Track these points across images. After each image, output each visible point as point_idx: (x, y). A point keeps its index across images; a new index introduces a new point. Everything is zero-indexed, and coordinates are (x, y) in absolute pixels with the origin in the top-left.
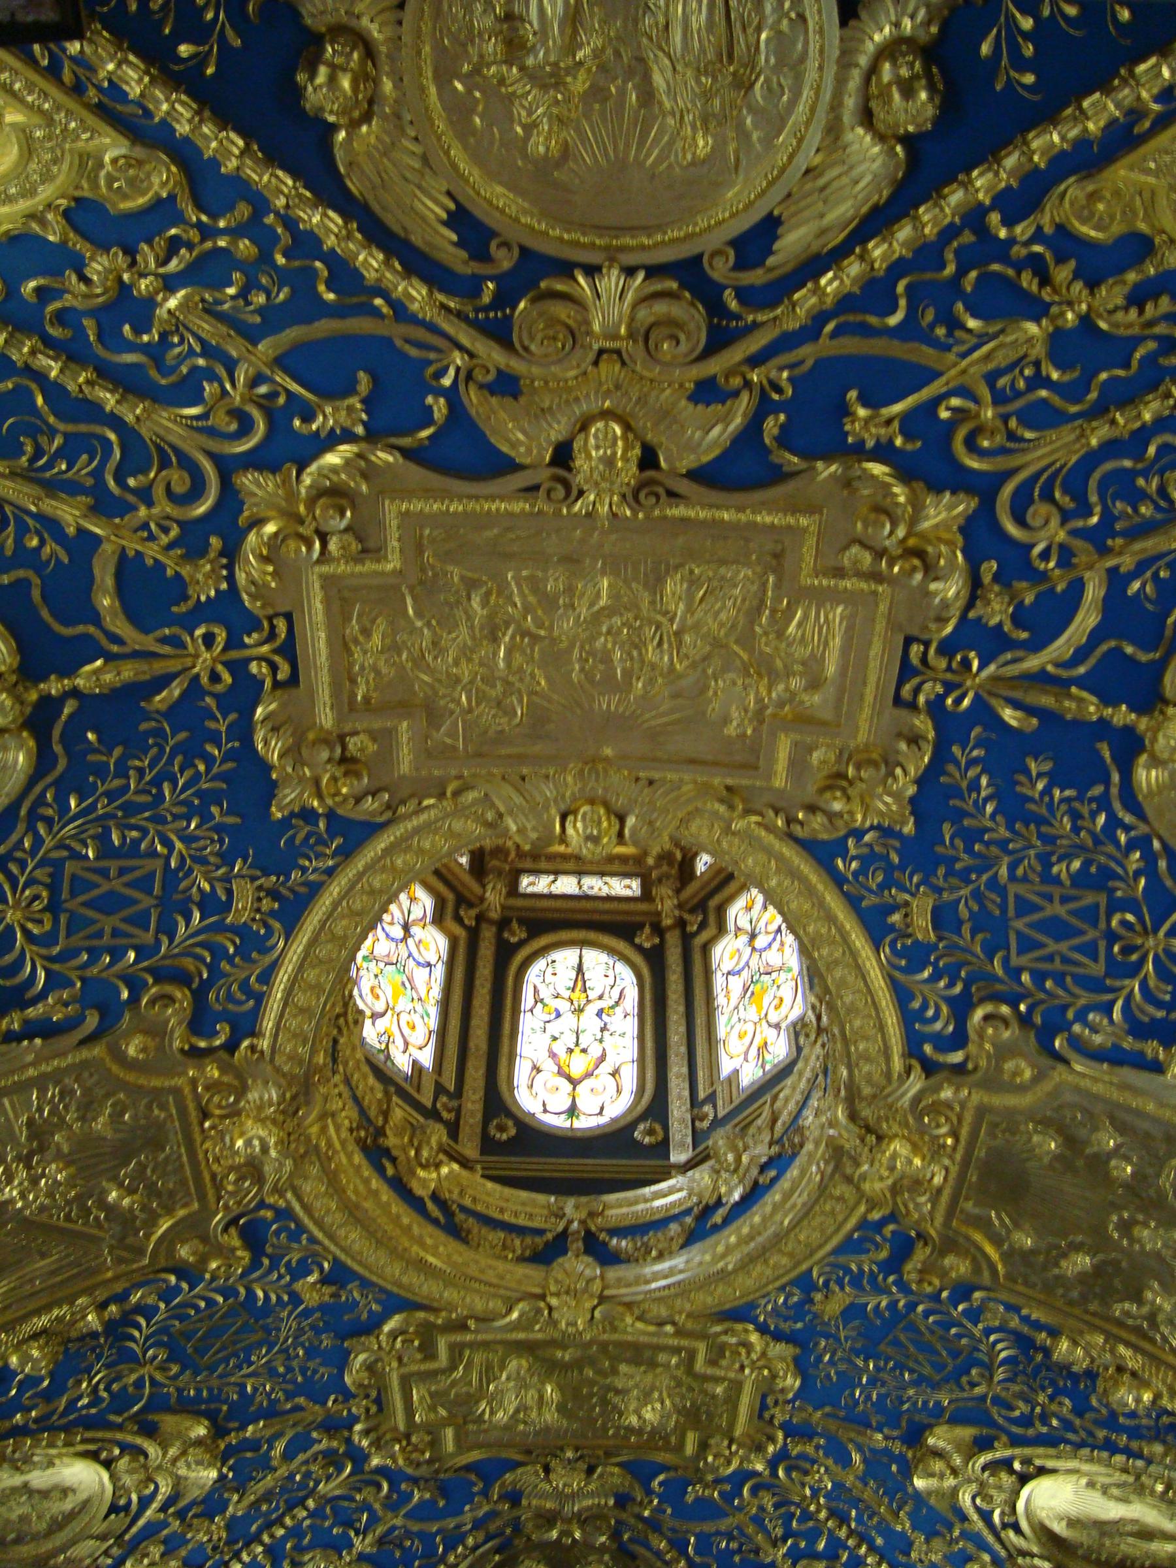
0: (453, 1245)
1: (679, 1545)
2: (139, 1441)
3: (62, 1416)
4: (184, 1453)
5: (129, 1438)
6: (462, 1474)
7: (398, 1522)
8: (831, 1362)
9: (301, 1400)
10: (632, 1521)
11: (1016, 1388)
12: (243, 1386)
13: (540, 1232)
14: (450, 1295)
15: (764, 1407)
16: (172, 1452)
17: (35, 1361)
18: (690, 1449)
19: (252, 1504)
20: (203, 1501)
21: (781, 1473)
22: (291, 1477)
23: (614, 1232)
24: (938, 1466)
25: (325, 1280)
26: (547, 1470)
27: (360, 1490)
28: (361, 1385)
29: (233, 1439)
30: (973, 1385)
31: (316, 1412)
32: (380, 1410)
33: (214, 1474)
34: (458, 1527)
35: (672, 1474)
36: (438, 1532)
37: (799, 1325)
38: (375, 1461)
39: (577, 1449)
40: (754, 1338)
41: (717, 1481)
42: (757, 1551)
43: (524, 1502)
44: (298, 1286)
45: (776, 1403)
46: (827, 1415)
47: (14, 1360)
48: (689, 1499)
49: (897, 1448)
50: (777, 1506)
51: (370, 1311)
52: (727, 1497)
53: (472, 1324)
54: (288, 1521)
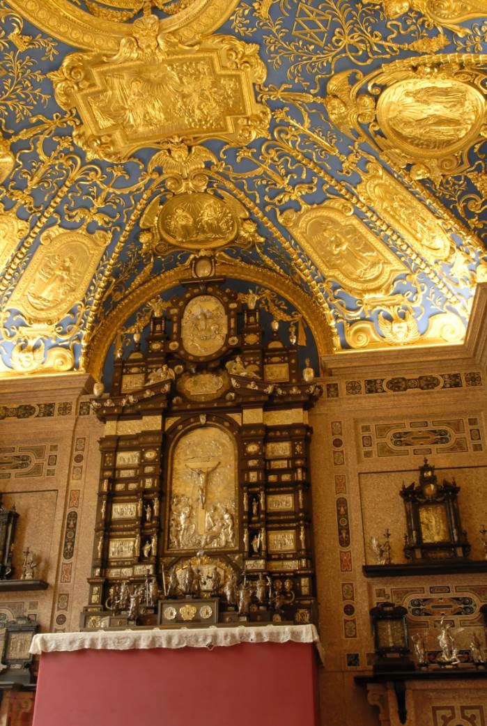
0: (83, 13)
1: (240, 186)
6: (132, 159)
7: (111, 190)
8: (276, 52)
9: (41, 118)
10: (215, 176)
11: (356, 35)
12: (6, 106)
13: (131, 10)
14: (87, 39)
15: (256, 94)
18: (231, 129)
19: (38, 183)
21: (275, 134)
22: (52, 167)
23: (164, 5)
24: (335, 102)
25: (23, 33)
26: (169, 151)
27: (88, 174)
28: (65, 104)
29: (14, 139)
30: (338, 41)
31: (52, 125)
32: (82, 123)
34: (137, 190)
35: (227, 147)
36: (131, 193)
37: (255, 29)
38: (90, 156)
39: (179, 137)
40: (237, 43)
41: (249, 147)
42: (276, 185)
43: (164, 171)
44: (11, 37)
45: (260, 89)
46: (285, 90)
48: (238, 160)
49: (319, 100)
50: (279, 157)
51: (53, 54)
52: (256, 156)
53: (105, 59)
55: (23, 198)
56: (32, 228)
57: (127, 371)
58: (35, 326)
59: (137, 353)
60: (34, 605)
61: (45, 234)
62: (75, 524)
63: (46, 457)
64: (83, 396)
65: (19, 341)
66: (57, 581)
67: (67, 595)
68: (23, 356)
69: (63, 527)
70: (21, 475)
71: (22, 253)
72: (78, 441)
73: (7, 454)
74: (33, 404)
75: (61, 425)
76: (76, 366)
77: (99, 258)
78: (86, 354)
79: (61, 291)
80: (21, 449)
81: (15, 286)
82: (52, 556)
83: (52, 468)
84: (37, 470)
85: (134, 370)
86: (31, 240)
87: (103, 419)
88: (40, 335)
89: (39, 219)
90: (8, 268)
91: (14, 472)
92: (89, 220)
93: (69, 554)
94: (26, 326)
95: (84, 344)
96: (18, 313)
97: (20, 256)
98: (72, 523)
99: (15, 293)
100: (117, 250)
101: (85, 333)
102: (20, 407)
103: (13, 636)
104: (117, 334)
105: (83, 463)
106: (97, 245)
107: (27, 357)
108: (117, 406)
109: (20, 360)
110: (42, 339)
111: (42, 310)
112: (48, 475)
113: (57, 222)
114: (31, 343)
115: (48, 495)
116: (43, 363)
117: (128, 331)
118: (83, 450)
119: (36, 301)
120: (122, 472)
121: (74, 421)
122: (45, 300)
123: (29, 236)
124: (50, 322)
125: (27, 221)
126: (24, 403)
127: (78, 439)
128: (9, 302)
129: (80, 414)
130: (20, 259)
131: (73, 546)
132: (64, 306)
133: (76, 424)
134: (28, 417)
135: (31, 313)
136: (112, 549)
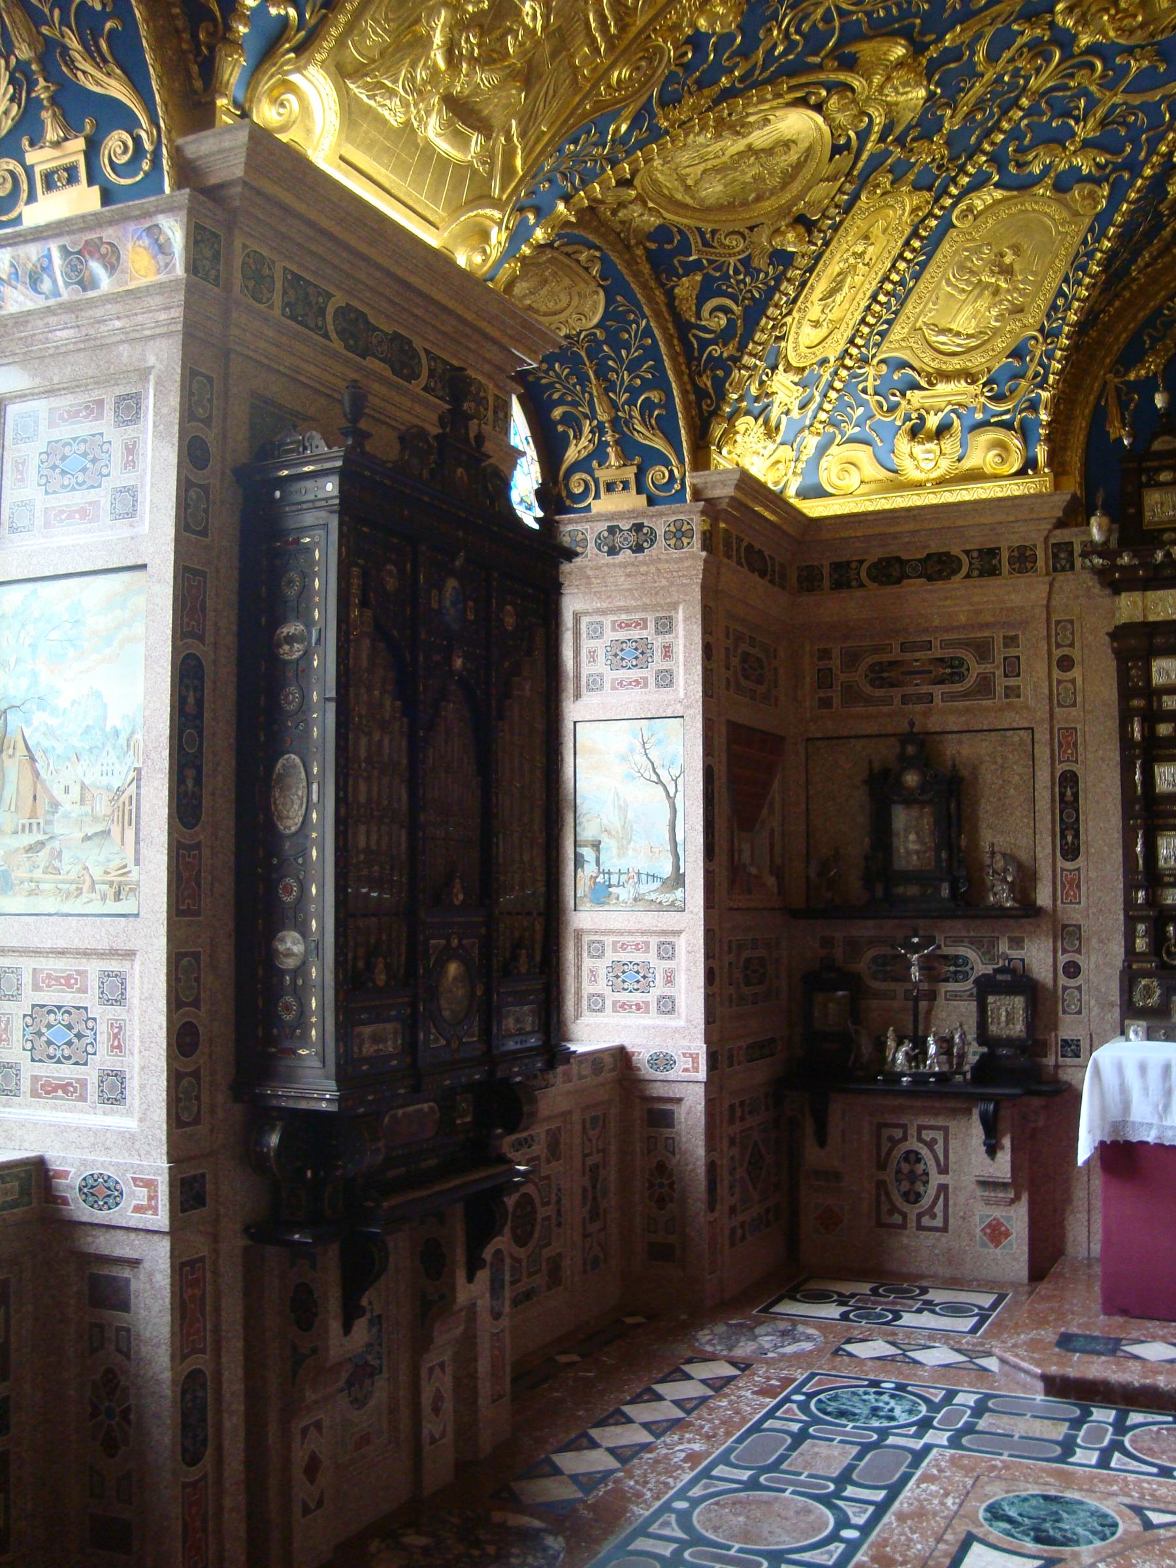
2: (842, 77)
3: (764, 68)
4: (888, 78)
5: (833, 76)
16: (877, 80)
17: (722, 17)
20: (917, 125)
33: (922, 93)
47: (702, 23)
54: (1005, 125)
55: (930, 152)
56: (936, 200)
57: (1150, 479)
58: (942, 387)
59: (1167, 438)
60: (1017, 943)
61: (962, 206)
62: (1076, 795)
63: (999, 658)
64: (1057, 532)
65: (908, 418)
66: (1055, 901)
67: (1079, 927)
68: (918, 449)
69: (1053, 801)
70: (953, 697)
71: (914, 250)
72: (1059, 629)
73: (918, 655)
74: (955, 551)
75: (1021, 594)
76: (1030, 464)
77: (1078, 240)
78: (1049, 439)
79: (994, 312)
80: (946, 644)
81: (896, 313)
82: (1039, 855)
83: (1012, 682)
84: (985, 687)
85: (1165, 476)
86: (934, 223)
87: (1116, 588)
88: (949, 403)
89: (954, 181)
90: (882, 282)
91: (938, 691)
92: (1061, 167)
93: (1071, 852)
94: (922, 388)
95: (1044, 417)
96: (905, 364)
97: (908, 255)
98: (1069, 792)
99: (897, 328)
100: (1119, 219)
101: (1045, 395)
102: (929, 556)
103: (991, 999)
104: (1105, 383)
105: (1076, 673)
106: (1076, 214)
107: (929, 452)
108: (1141, 565)
109: (911, 455)
110: (953, 411)
111: (954, 354)
112: (1007, 696)
113: (989, 177)
114: (932, 422)
115: (1016, 737)
116: (959, 460)
117: (1132, 376)
118: (1072, 645)
119: (942, 338)
120: (1165, 698)
121: (1047, 587)
122: (958, 334)
123: (931, 214)
124: (970, 377)
125: (929, 189)
126: (934, 547)
127: (1058, 622)
128: (884, 347)
129: (1055, 570)
130: (908, 262)
131: (1077, 836)
132: (1002, 344)
133: (1050, 593)
134: (948, 577)
135: (931, 362)
136: (1163, 852)
